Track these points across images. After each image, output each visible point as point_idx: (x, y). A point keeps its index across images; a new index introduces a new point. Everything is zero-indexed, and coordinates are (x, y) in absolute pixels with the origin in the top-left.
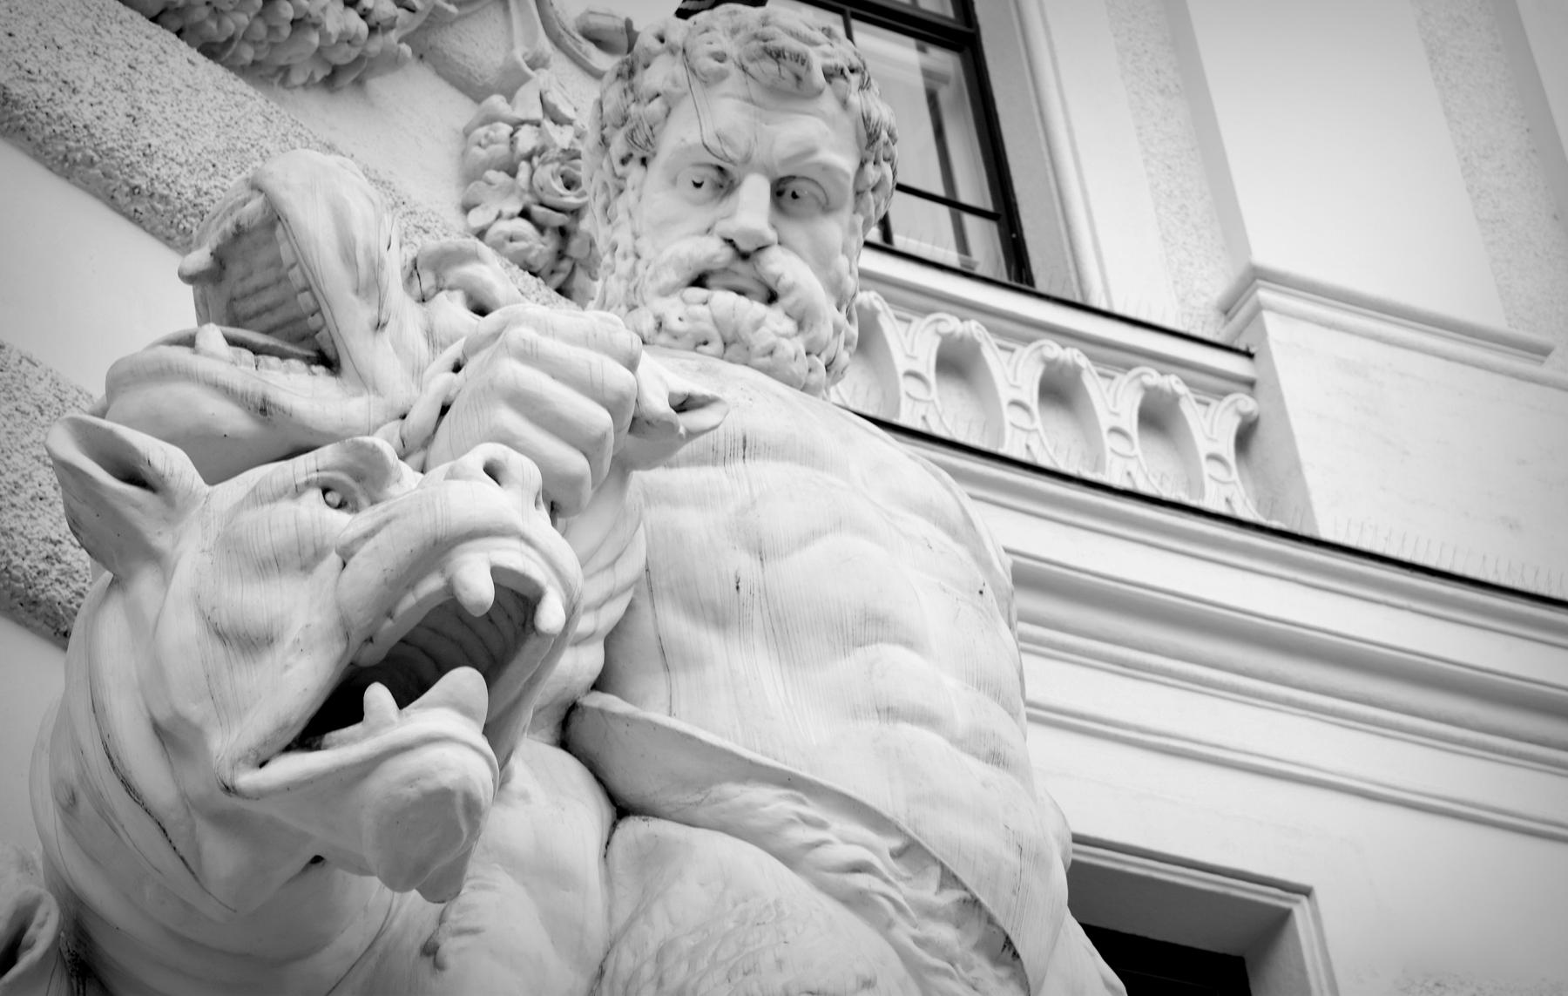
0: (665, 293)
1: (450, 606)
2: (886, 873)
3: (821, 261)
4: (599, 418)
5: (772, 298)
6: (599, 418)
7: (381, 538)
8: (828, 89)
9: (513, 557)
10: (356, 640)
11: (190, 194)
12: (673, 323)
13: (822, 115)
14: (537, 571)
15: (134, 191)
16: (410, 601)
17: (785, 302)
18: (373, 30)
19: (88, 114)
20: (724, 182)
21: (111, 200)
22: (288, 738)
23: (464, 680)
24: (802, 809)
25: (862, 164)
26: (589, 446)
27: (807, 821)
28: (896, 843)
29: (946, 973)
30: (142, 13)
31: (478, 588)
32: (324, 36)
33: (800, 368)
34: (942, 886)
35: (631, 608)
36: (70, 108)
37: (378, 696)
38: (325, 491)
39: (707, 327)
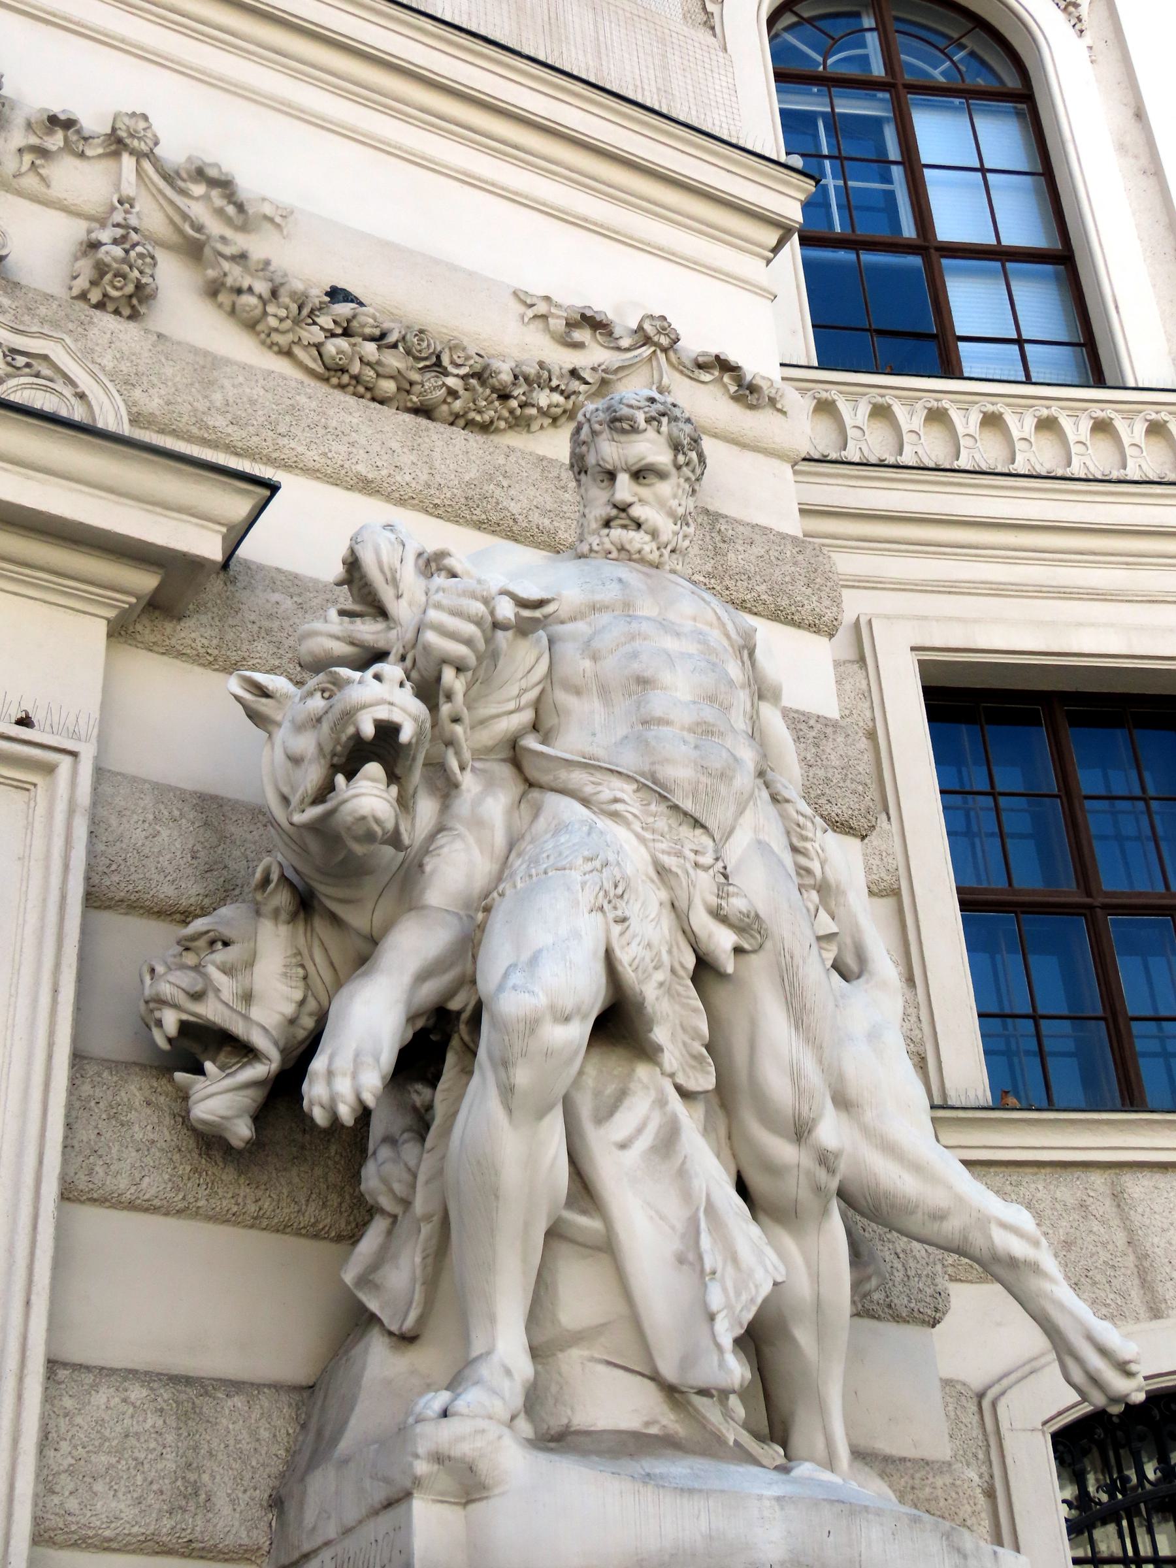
0: (593, 533)
1: (357, 737)
3: (661, 503)
5: (639, 525)
7: (330, 715)
8: (649, 427)
9: (383, 713)
10: (329, 757)
12: (595, 548)
13: (648, 441)
14: (397, 716)
15: (436, 506)
16: (344, 738)
17: (643, 527)
18: (567, 398)
20: (611, 476)
23: (374, 769)
24: (592, 779)
25: (676, 456)
26: (469, 642)
27: (593, 783)
29: (658, 841)
30: (443, 421)
32: (540, 409)
35: (542, 692)
36: (398, 478)
38: (323, 691)
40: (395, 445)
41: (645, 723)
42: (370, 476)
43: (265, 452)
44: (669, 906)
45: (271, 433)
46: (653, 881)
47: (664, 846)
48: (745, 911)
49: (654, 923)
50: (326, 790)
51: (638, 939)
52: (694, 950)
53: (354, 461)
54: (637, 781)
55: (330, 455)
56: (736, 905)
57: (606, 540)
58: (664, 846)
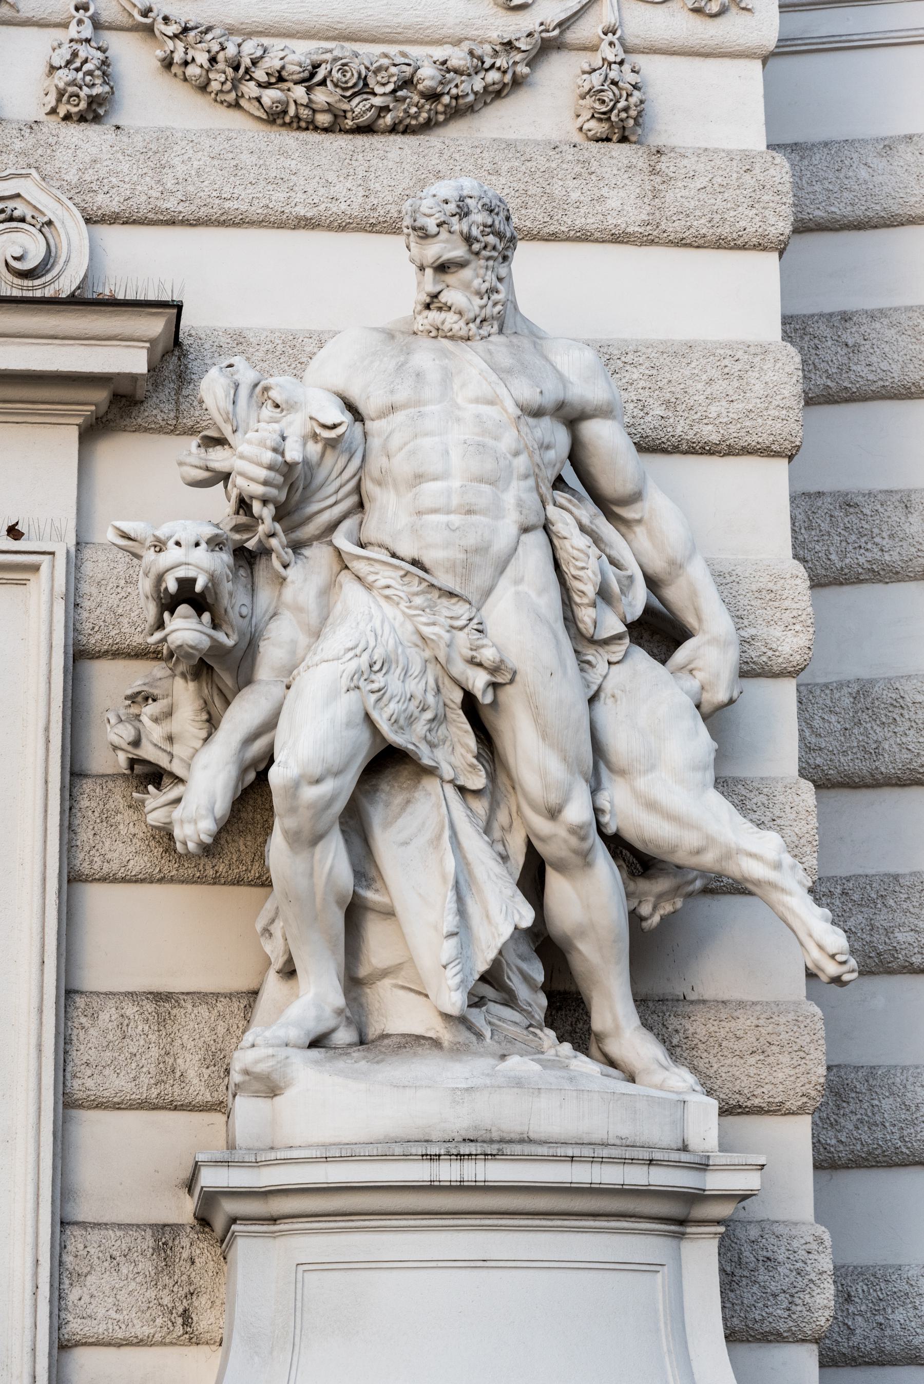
2: (397, 586)
4: (263, 473)
6: (263, 473)
11: (396, 215)
17: (453, 309)
19: (343, 206)
21: (364, 230)
22: (155, 627)
28: (402, 573)
31: (172, 586)
33: (463, 333)
34: (420, 583)
36: (334, 209)
37: (166, 615)
38: (155, 546)
39: (429, 327)
40: (332, 177)
41: (419, 513)
42: (309, 215)
43: (214, 218)
44: (434, 660)
45: (217, 201)
46: (417, 646)
47: (423, 619)
48: (491, 658)
49: (417, 679)
50: (160, 625)
51: (397, 699)
52: (463, 689)
53: (293, 204)
54: (402, 569)
55: (271, 206)
56: (488, 655)
57: (426, 321)
58: (423, 619)
